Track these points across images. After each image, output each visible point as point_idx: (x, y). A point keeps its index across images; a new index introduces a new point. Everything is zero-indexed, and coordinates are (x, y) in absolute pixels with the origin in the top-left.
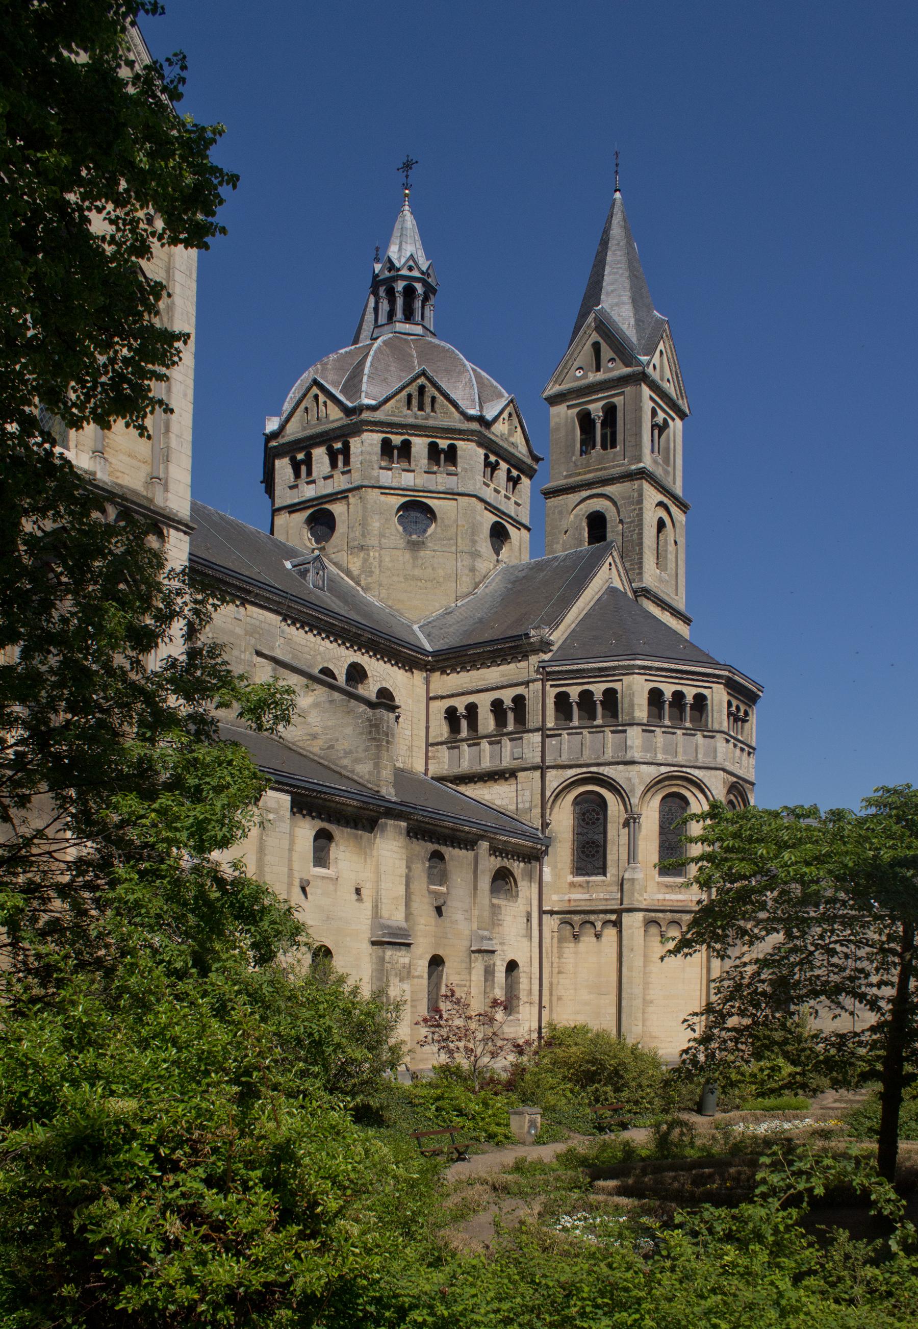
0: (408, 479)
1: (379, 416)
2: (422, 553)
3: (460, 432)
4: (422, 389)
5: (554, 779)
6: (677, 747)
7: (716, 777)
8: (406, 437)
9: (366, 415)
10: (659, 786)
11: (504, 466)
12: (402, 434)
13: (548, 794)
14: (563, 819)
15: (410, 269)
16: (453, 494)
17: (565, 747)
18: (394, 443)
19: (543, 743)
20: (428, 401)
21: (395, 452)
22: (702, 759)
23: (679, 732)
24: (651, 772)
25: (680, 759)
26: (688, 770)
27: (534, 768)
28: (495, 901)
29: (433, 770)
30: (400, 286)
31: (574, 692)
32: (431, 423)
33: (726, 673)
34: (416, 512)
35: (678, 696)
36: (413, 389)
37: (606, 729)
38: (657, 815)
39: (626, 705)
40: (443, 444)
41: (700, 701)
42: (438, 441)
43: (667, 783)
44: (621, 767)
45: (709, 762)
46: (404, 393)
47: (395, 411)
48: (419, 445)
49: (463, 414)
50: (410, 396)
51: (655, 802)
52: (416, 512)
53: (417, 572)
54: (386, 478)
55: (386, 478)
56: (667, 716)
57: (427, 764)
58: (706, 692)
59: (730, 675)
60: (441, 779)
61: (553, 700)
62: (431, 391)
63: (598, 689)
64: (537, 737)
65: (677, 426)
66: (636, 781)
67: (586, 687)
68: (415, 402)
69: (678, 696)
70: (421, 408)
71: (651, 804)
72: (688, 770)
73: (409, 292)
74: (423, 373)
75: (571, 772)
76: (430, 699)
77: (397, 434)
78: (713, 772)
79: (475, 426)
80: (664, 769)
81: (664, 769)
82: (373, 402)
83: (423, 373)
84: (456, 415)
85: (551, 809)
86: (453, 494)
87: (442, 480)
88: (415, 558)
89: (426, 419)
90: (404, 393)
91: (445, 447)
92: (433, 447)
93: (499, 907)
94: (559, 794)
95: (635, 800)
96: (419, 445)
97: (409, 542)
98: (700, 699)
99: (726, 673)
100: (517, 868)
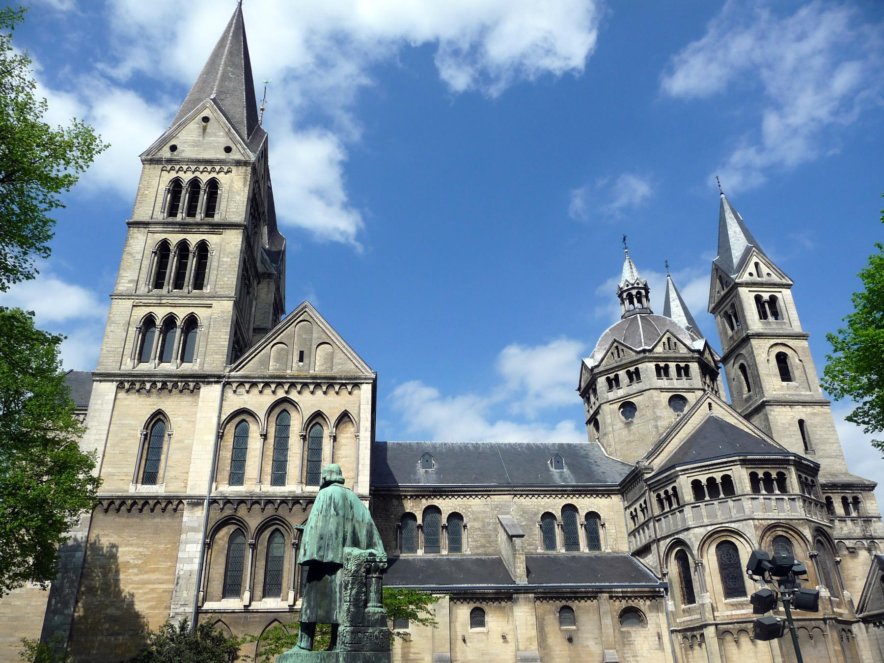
0: (620, 393)
1: (601, 369)
2: (633, 427)
3: (637, 360)
4: (617, 347)
5: (664, 545)
6: (719, 512)
7: (747, 525)
9: (596, 371)
10: (711, 539)
11: (672, 366)
14: (673, 568)
15: (628, 286)
16: (641, 392)
17: (664, 525)
20: (620, 352)
21: (613, 383)
22: (735, 515)
23: (716, 502)
24: (702, 531)
25: (720, 520)
26: (727, 525)
30: (625, 295)
32: (623, 362)
33: (737, 458)
34: (628, 408)
35: (711, 481)
36: (613, 349)
38: (715, 558)
41: (727, 479)
43: (716, 536)
44: (686, 533)
45: (740, 516)
48: (622, 374)
49: (636, 352)
52: (628, 408)
53: (632, 438)
54: (611, 396)
55: (611, 396)
56: (721, 492)
58: (728, 473)
59: (741, 458)
62: (620, 347)
65: (785, 297)
66: (693, 539)
68: (616, 355)
69: (711, 481)
71: (709, 552)
72: (727, 525)
73: (630, 297)
74: (615, 341)
75: (668, 540)
78: (744, 522)
79: (642, 355)
81: (710, 528)
83: (615, 341)
84: (634, 353)
85: (667, 563)
86: (641, 392)
87: (636, 387)
88: (629, 431)
90: (609, 353)
92: (628, 373)
94: (667, 555)
95: (695, 552)
96: (622, 374)
97: (626, 424)
99: (737, 458)
100: (643, 605)
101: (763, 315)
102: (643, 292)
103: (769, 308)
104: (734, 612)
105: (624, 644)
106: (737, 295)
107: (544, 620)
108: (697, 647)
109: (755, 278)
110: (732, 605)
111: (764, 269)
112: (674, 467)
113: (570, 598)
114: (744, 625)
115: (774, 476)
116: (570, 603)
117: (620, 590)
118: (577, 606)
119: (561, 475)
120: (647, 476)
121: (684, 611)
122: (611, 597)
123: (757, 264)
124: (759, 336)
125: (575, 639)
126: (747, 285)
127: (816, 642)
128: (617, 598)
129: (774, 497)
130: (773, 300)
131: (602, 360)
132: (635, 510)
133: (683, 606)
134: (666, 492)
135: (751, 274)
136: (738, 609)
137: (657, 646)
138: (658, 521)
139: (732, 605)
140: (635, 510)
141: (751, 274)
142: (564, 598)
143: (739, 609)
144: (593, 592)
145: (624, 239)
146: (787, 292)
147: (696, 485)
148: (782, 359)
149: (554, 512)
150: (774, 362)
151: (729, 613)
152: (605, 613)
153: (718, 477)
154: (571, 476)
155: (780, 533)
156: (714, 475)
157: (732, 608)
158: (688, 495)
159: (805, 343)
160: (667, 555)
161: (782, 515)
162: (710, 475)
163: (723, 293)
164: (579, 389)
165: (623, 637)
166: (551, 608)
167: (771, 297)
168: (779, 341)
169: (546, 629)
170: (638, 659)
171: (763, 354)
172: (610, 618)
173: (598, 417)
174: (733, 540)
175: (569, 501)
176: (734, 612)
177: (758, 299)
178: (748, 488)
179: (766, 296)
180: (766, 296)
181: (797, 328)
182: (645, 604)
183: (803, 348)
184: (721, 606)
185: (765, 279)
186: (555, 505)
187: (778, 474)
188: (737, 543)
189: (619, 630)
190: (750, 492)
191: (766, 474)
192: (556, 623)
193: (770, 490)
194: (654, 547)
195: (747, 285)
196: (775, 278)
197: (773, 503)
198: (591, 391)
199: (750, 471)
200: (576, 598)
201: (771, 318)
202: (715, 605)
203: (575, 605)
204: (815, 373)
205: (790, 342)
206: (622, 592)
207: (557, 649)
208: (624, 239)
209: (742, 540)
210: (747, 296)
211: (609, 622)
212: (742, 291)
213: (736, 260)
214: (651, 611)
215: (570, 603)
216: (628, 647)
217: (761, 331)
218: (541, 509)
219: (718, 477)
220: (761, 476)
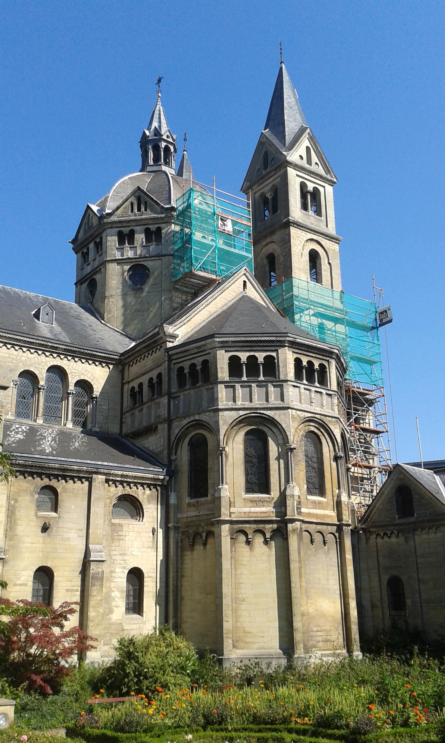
1: (114, 218)
5: (177, 427)
8: (132, 228)
12: (129, 226)
13: (173, 438)
14: (183, 456)
18: (124, 233)
19: (169, 403)
27: (164, 421)
28: (116, 521)
29: (126, 430)
31: (186, 365)
35: (252, 359)
37: (202, 388)
39: (213, 370)
40: (153, 228)
42: (150, 226)
46: (128, 203)
47: (126, 214)
50: (132, 204)
51: (240, 437)
57: (121, 427)
60: (127, 436)
61: (176, 373)
63: (198, 361)
64: (165, 400)
65: (328, 192)
67: (193, 361)
69: (252, 359)
70: (139, 210)
71: (236, 439)
76: (123, 384)
77: (126, 227)
80: (242, 413)
81: (242, 413)
82: (110, 211)
89: (142, 215)
90: (128, 203)
91: (155, 230)
93: (120, 525)
98: (269, 360)
101: (305, 207)
102: (172, 148)
103: (311, 199)
104: (253, 510)
105: (113, 539)
106: (285, 176)
107: (16, 501)
108: (199, 548)
109: (304, 163)
110: (252, 501)
111: (314, 158)
112: (212, 336)
113: (56, 477)
114: (261, 526)
115: (316, 366)
116: (54, 483)
117: (120, 473)
118: (63, 488)
119: (51, 330)
120: (169, 345)
121: (189, 505)
122: (107, 481)
123: (308, 148)
124: (299, 225)
125: (53, 529)
126: (296, 167)
127: (328, 549)
128: (114, 482)
129: (313, 389)
130: (315, 194)
131: (118, 208)
132: (141, 385)
133: (187, 500)
134: (193, 366)
135: (301, 157)
136: (257, 506)
137: (150, 544)
138: (174, 398)
139: (252, 501)
140: (141, 385)
141: (301, 157)
142: (48, 476)
143: (260, 507)
144: (87, 472)
145: (159, 81)
146: (329, 189)
147: (234, 362)
148: (314, 257)
149: (37, 372)
150: (306, 258)
151: (247, 510)
152: (98, 499)
153: (261, 356)
154: (63, 334)
155: (313, 429)
156: (257, 354)
157: (251, 504)
158: (223, 372)
159: (336, 247)
160: (180, 439)
161: (318, 410)
162: (252, 354)
163: (264, 172)
164: (73, 242)
165: (113, 531)
166: (27, 488)
167: (315, 188)
168: (315, 237)
169: (17, 513)
170: (127, 558)
171: (300, 244)
172: (102, 504)
173: (98, 277)
174: (265, 429)
175: (57, 362)
176: (253, 510)
177: (303, 186)
178: (291, 374)
179: (310, 186)
180: (310, 186)
181: (332, 230)
182: (144, 493)
183: (334, 250)
184: (239, 502)
185: (313, 168)
186: (40, 364)
187: (322, 366)
188: (269, 432)
189: (110, 521)
190: (293, 379)
191: (310, 363)
192: (33, 507)
193: (311, 380)
194: (163, 428)
195: (296, 167)
196: (321, 170)
197: (313, 394)
198: (92, 246)
199: (296, 356)
200: (64, 478)
201: (311, 213)
202: (232, 500)
203: (60, 485)
204: (340, 280)
205: (325, 242)
206: (122, 476)
207: (29, 540)
208: (159, 81)
209: (275, 430)
210: (294, 179)
211: (101, 509)
212: (291, 172)
213: (289, 138)
214: (149, 502)
215: (54, 483)
216: (117, 543)
217: (301, 221)
218: (21, 365)
219: (261, 356)
220: (305, 363)
